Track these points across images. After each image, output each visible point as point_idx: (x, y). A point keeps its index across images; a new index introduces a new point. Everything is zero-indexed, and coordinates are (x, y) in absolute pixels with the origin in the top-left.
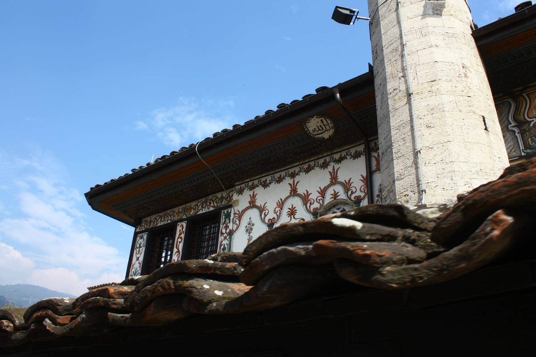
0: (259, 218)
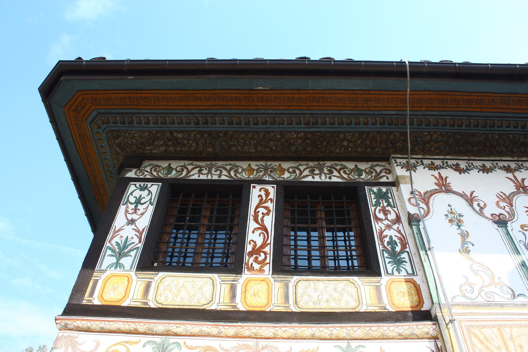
0: (469, 209)
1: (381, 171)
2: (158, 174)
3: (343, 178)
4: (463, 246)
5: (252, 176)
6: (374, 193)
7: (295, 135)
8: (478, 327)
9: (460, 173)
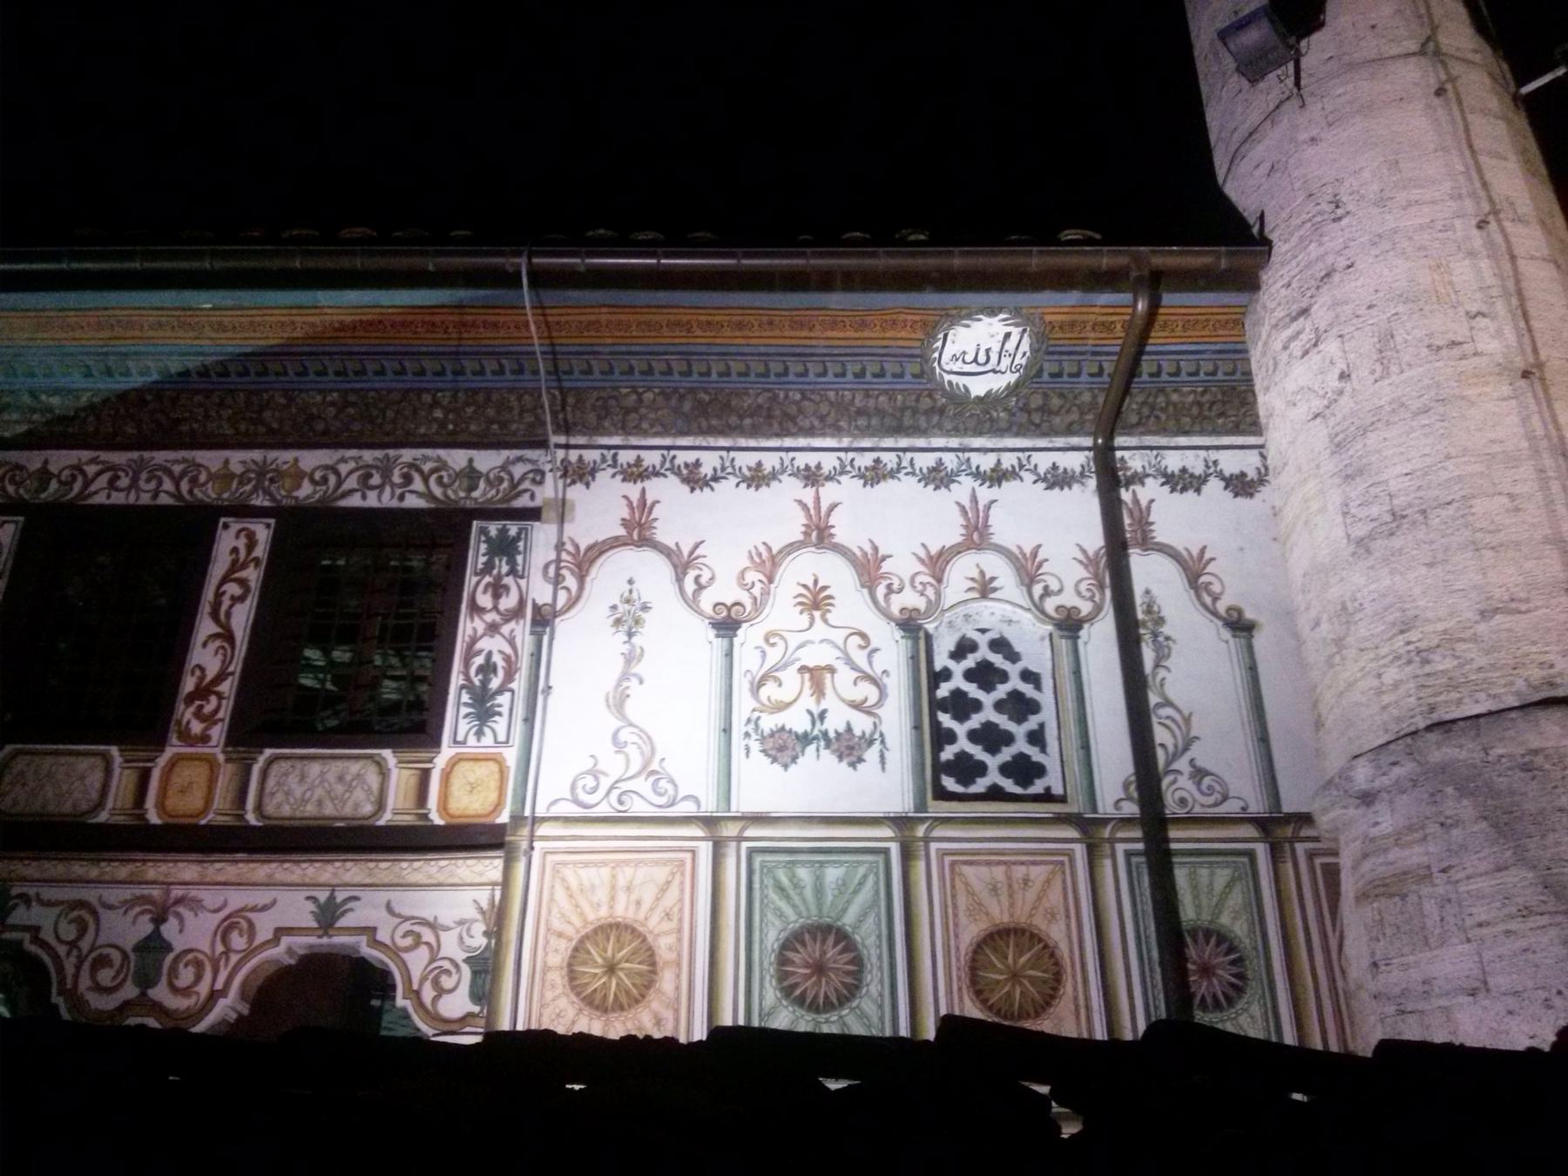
0: (672, 588)
1: (523, 478)
2: (17, 491)
3: (429, 496)
4: (618, 685)
5: (226, 496)
6: (489, 540)
7: (319, 398)
8: (575, 863)
9: (693, 490)
